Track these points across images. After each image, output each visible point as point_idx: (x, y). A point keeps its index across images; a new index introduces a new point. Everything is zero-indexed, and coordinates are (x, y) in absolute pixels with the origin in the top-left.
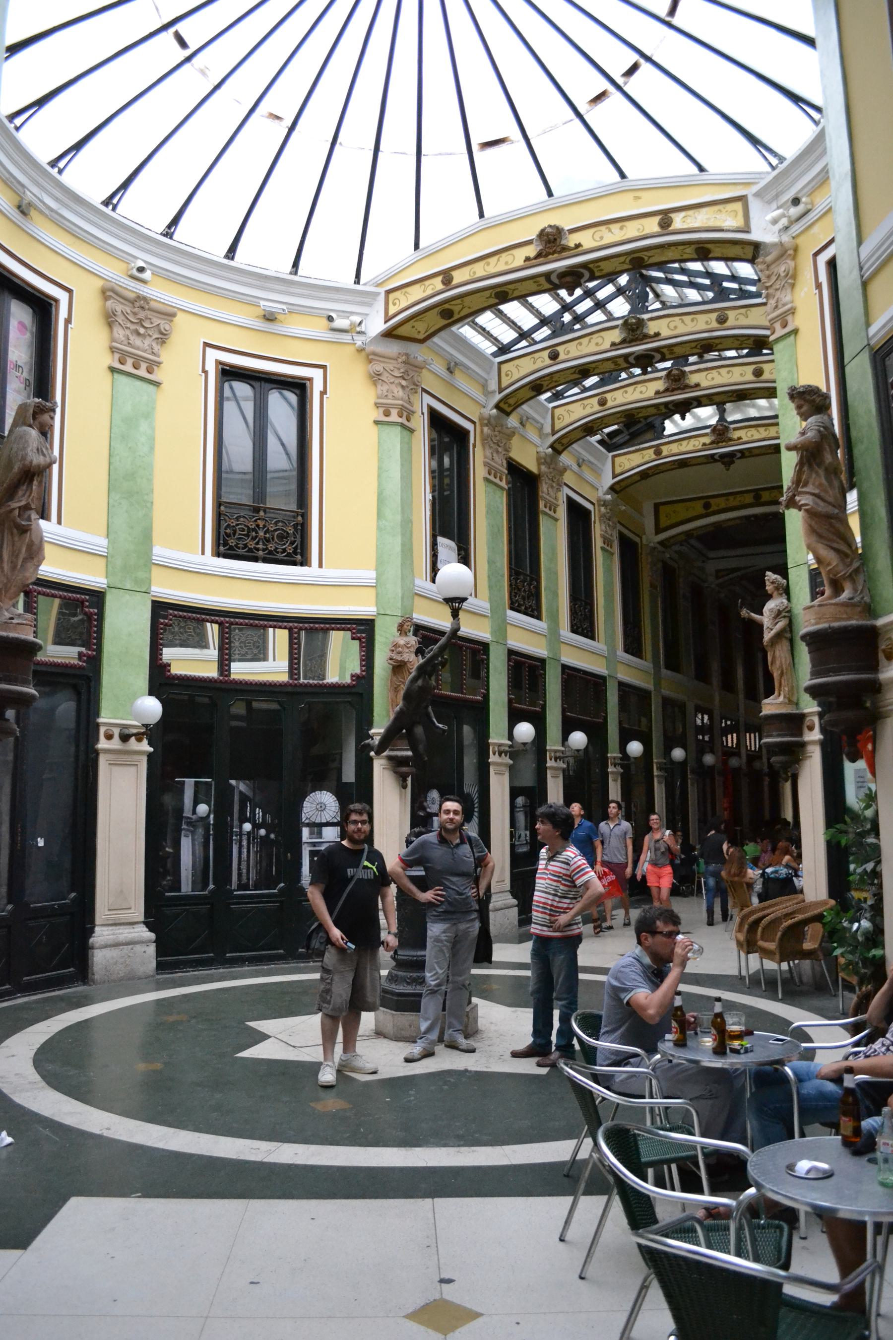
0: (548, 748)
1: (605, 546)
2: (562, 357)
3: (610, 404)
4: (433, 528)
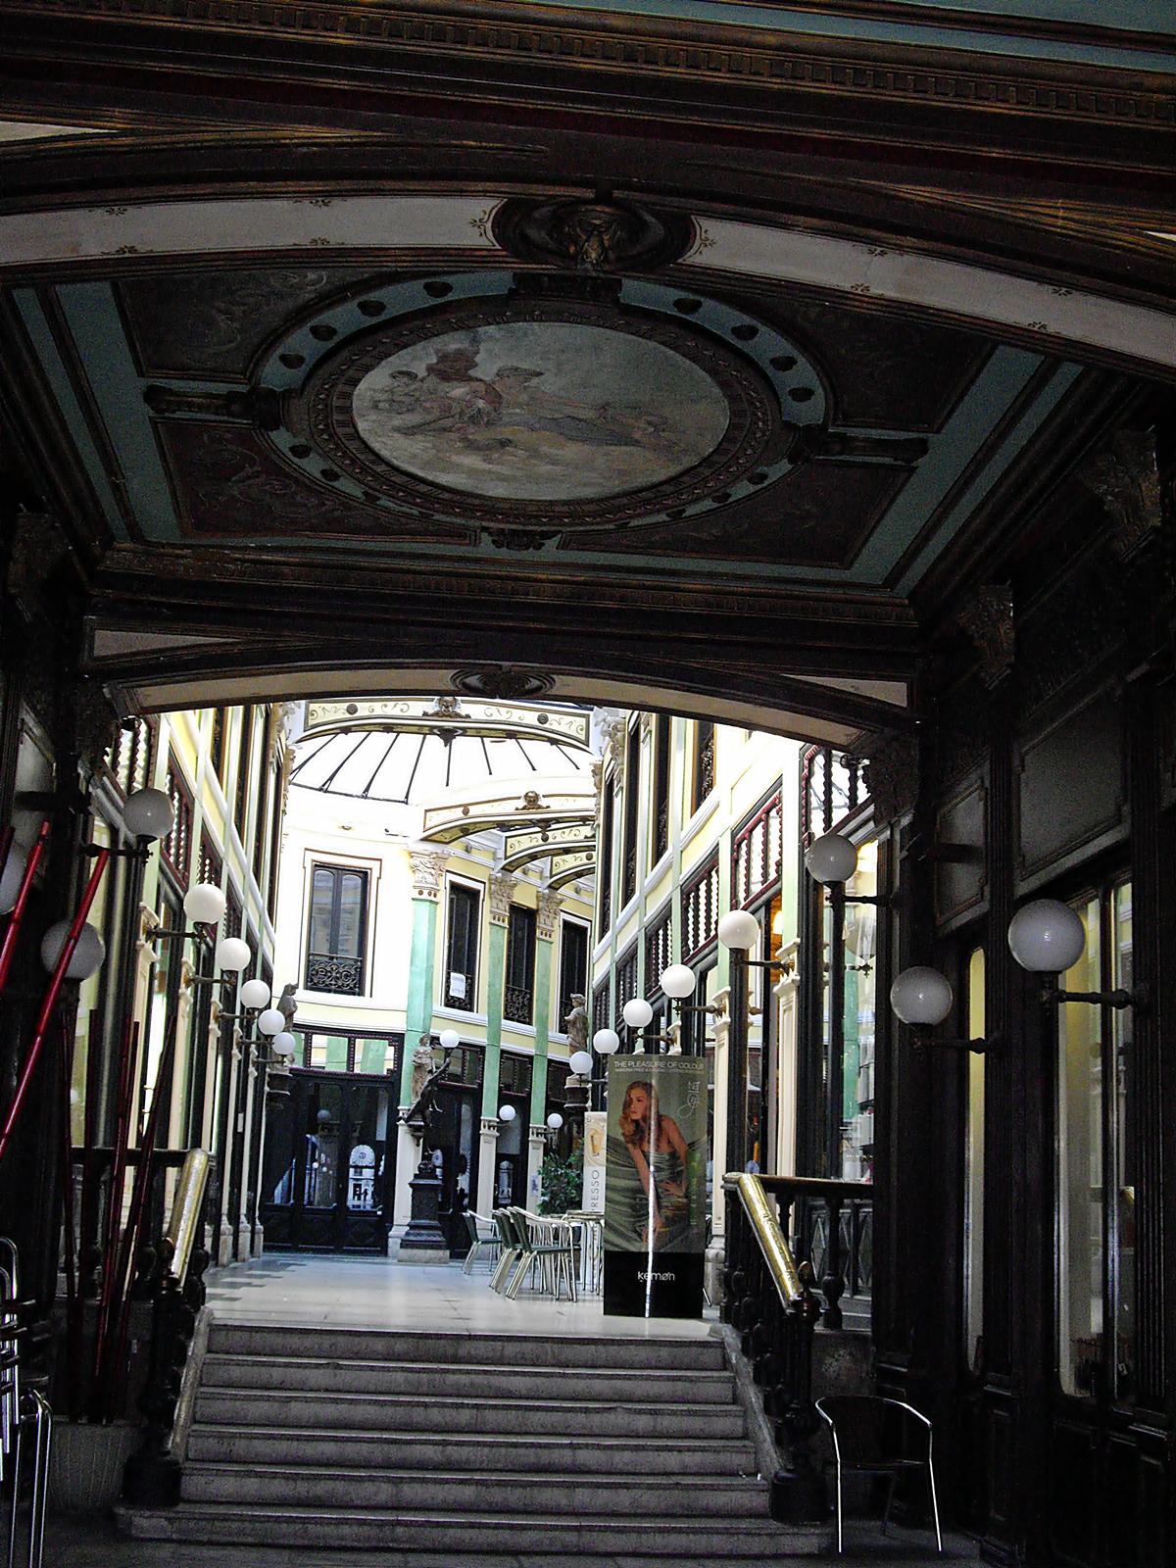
2: (550, 840)
4: (449, 967)
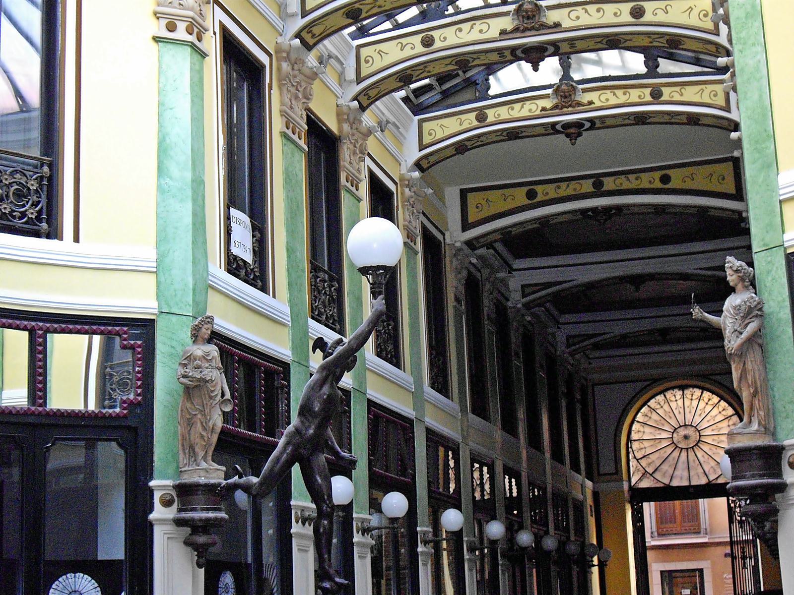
0: (354, 515)
1: (409, 241)
3: (438, 44)
